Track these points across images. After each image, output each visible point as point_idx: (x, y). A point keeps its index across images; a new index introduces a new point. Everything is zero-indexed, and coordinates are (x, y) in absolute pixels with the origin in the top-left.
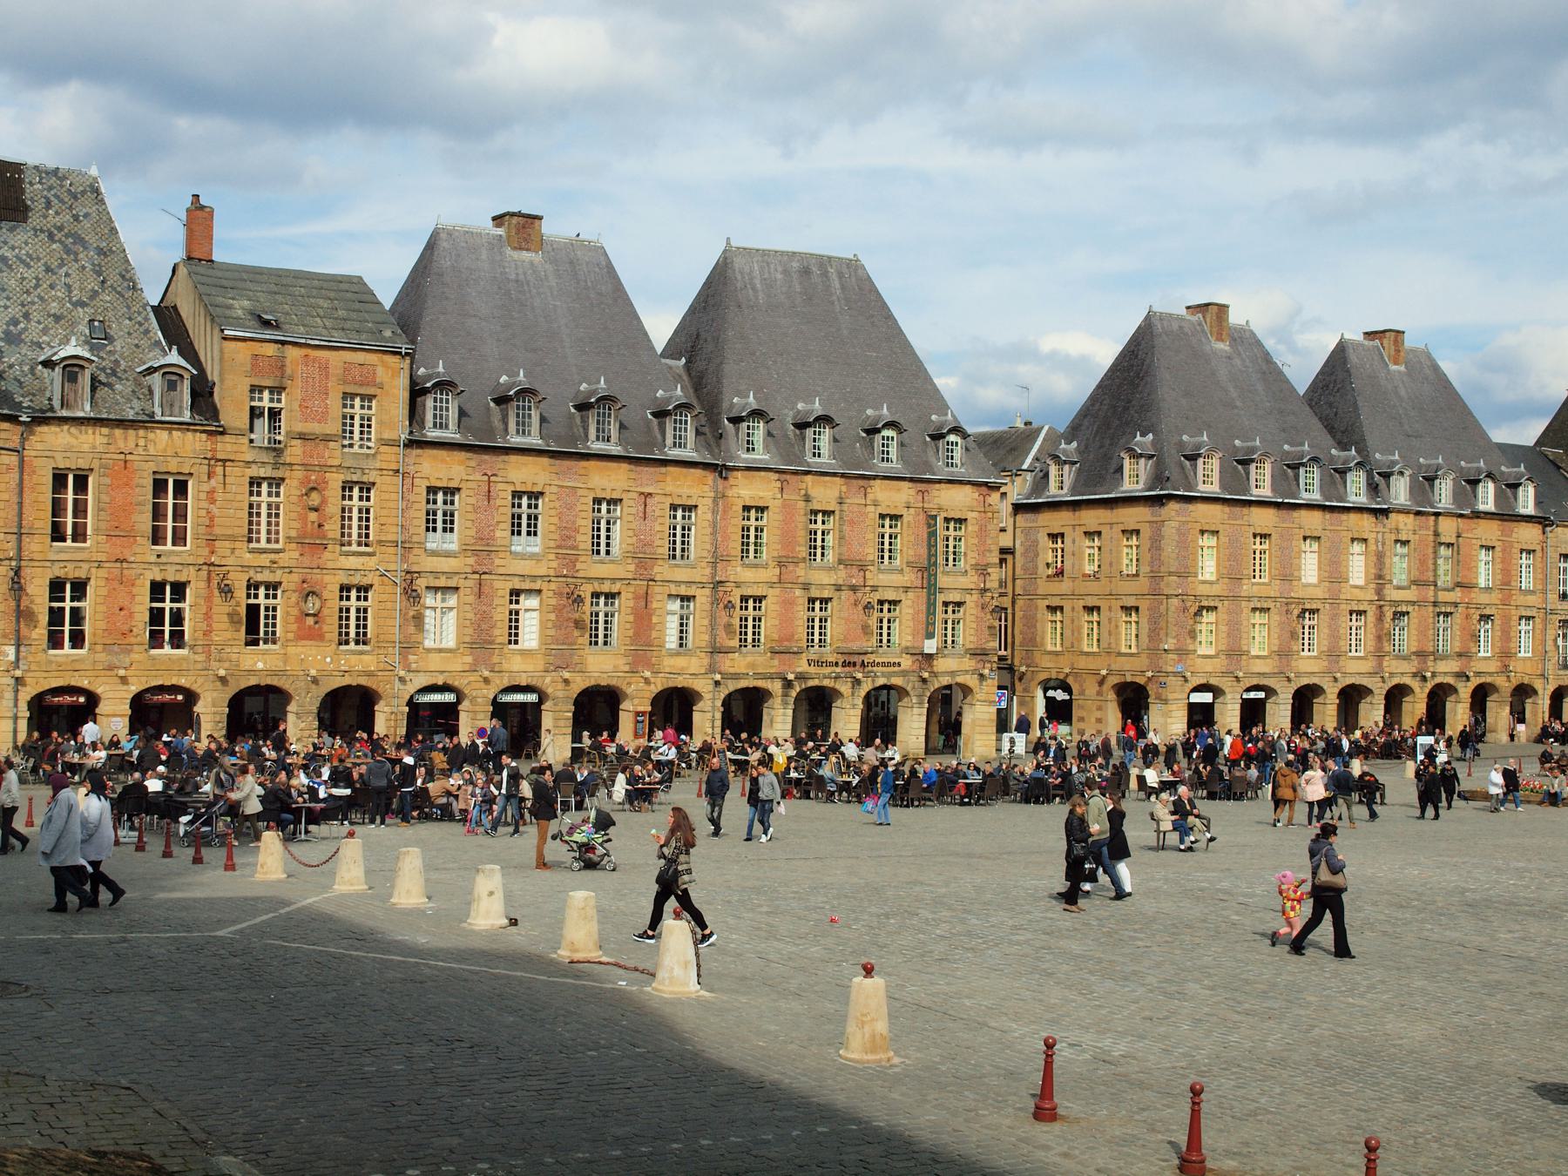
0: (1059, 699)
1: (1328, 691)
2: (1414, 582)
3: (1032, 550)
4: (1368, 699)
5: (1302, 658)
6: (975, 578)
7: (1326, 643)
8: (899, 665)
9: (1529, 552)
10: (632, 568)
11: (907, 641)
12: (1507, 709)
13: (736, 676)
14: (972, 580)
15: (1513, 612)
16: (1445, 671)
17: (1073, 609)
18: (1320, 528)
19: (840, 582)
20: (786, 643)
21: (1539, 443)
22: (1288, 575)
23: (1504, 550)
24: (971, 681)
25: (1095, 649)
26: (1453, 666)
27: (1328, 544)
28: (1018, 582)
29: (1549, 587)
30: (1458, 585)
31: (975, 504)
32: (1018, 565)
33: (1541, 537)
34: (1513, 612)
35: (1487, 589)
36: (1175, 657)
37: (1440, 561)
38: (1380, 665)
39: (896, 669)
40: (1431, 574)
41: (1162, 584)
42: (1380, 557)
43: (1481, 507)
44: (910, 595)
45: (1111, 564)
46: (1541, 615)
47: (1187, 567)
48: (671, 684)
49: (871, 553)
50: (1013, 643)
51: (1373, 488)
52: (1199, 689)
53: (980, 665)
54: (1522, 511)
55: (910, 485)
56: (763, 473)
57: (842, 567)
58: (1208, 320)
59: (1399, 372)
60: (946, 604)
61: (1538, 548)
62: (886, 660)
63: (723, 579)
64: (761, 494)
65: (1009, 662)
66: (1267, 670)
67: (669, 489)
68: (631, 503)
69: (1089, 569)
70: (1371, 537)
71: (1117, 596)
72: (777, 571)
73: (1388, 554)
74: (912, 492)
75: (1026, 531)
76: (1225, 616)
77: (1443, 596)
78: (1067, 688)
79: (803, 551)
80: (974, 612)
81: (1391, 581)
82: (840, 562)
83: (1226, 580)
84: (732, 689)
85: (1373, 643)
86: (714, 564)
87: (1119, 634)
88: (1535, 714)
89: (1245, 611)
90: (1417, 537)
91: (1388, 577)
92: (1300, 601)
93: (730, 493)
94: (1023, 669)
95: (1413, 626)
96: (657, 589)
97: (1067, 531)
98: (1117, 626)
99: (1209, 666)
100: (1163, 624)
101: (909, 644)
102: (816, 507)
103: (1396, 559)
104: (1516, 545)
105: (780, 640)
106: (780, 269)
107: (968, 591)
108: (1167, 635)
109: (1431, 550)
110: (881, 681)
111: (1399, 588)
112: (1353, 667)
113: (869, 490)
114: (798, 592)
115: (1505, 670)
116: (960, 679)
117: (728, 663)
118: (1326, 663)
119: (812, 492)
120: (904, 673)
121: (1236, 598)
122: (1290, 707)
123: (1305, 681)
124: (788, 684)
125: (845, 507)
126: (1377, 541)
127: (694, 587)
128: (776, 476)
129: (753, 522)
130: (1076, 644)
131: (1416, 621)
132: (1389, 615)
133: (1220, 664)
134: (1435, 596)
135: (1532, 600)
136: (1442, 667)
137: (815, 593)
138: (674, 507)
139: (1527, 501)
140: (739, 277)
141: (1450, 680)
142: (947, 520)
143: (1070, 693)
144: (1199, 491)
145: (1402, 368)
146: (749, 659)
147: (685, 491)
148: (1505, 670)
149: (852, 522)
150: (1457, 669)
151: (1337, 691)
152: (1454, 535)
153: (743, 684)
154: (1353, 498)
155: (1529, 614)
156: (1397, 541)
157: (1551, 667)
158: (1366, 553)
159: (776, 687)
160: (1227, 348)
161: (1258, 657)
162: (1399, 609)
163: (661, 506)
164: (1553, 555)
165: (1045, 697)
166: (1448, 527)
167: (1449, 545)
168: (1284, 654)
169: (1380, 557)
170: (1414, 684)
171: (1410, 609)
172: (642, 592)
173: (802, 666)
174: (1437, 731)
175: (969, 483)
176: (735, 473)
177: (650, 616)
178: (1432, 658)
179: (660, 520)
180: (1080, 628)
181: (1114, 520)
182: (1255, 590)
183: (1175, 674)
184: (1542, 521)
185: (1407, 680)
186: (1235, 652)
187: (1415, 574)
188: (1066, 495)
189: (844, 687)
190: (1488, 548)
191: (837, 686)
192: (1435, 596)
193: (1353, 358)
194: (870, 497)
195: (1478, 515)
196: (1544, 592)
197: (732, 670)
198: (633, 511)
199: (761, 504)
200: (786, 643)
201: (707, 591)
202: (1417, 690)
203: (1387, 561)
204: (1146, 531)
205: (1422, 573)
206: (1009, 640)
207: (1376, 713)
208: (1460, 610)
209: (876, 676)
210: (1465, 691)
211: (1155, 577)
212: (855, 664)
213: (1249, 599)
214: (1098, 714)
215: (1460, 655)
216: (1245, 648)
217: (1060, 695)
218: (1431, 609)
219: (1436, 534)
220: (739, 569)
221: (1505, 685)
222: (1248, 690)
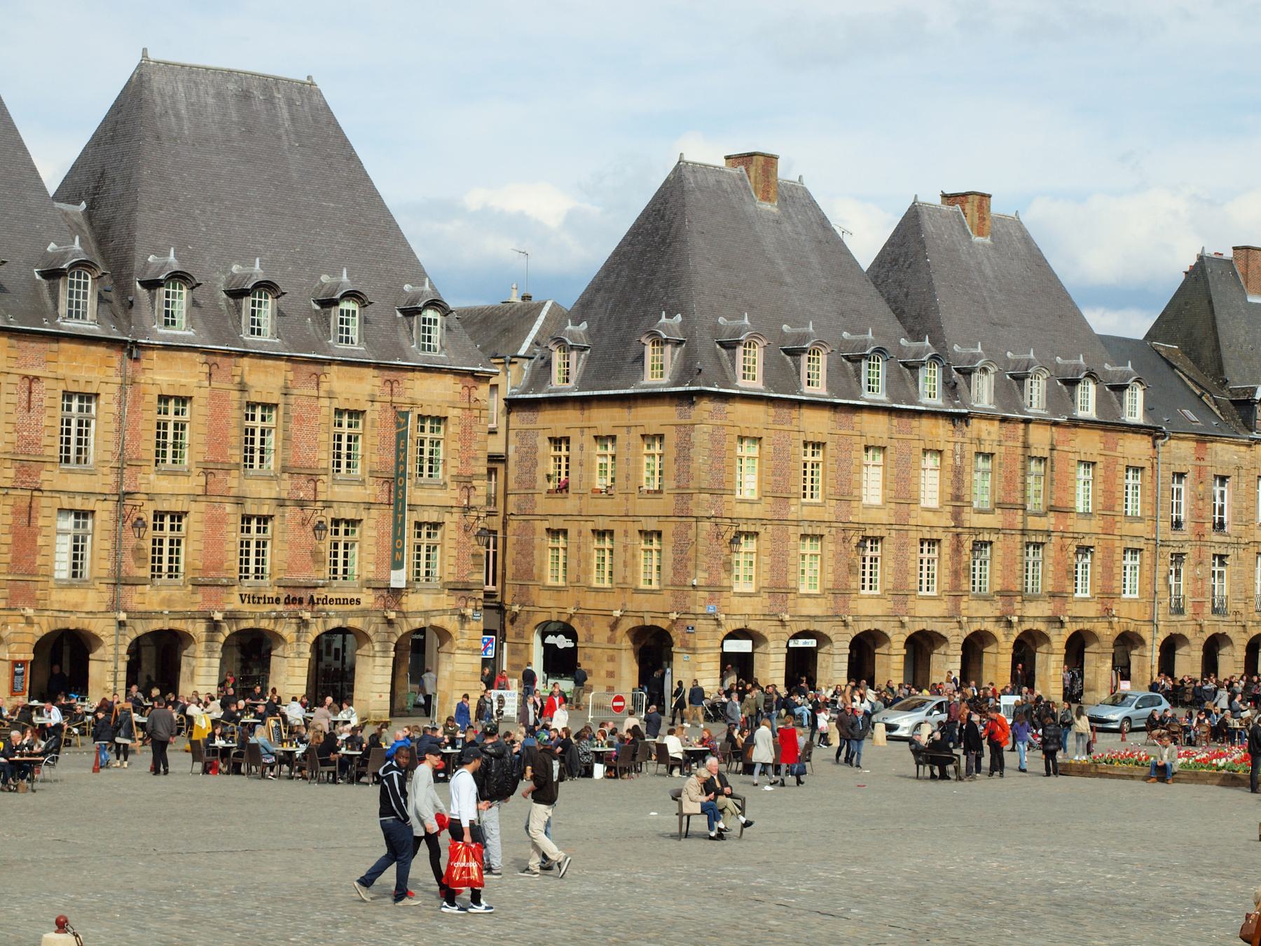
0: (561, 646)
1: (893, 639)
2: (999, 505)
3: (530, 458)
4: (942, 649)
5: (862, 597)
6: (457, 493)
7: (891, 579)
8: (358, 602)
9: (1136, 469)
10: (11, 473)
11: (369, 571)
12: (1109, 663)
13: (147, 616)
14: (451, 495)
15: (1117, 543)
16: (1035, 614)
17: (580, 533)
18: (885, 436)
19: (284, 495)
20: (212, 573)
21: (1150, 336)
22: (846, 494)
23: (1106, 467)
24: (450, 623)
25: (607, 584)
26: (1044, 609)
27: (895, 457)
28: (511, 498)
29: (1160, 513)
30: (1052, 509)
31: (458, 398)
32: (511, 477)
33: (1151, 452)
34: (1117, 543)
35: (1087, 514)
36: (706, 595)
37: (1030, 480)
39: (355, 607)
40: (1019, 495)
41: (691, 504)
42: (958, 473)
43: (1080, 414)
44: (374, 512)
45: (627, 478)
46: (1151, 547)
47: (721, 482)
48: (61, 625)
49: (324, 458)
50: (504, 575)
51: (951, 388)
52: (733, 635)
53: (461, 604)
54: (1129, 419)
55: (376, 372)
56: (185, 354)
57: (286, 476)
58: (752, 174)
59: (984, 245)
60: (419, 525)
61: (1147, 465)
62: (341, 596)
63: (131, 489)
64: (183, 381)
65: (499, 599)
67: (61, 372)
68: (11, 389)
69: (601, 483)
70: (947, 448)
71: (635, 518)
72: (202, 480)
73: (967, 469)
74: (378, 382)
75: (521, 435)
76: (768, 545)
77: (1034, 523)
78: (571, 633)
79: (236, 455)
80: (454, 535)
81: (970, 504)
82: (284, 469)
83: (770, 500)
84: (140, 631)
86: (120, 470)
87: (637, 565)
88: (1142, 669)
90: (1003, 448)
91: (967, 498)
92: (860, 526)
93: (142, 378)
94: (516, 608)
95: (997, 559)
96: (45, 502)
97: (574, 435)
98: (634, 556)
99: (748, 606)
100: (691, 553)
101: (371, 576)
102: (255, 398)
103: (977, 476)
104: (1121, 461)
105: (205, 570)
106: (212, 91)
107: (448, 508)
108: (696, 567)
109: (1019, 465)
110: (335, 623)
111: (980, 512)
112: (923, 609)
113: (322, 378)
114: (229, 508)
115: (1107, 614)
116: (436, 621)
117: (136, 598)
118: (891, 605)
119: (250, 380)
120: (365, 613)
121: (782, 521)
122: (846, 658)
123: (865, 626)
124: (214, 626)
125: (292, 400)
126: (954, 452)
127: (93, 499)
128: (203, 358)
129: (171, 417)
130: (582, 578)
131: (1000, 552)
132: (968, 545)
133: (761, 604)
134: (1024, 522)
135: (1139, 528)
136: (1032, 610)
137: (251, 509)
138: (68, 396)
139: (1134, 408)
140: (158, 100)
141: (1041, 626)
142: (422, 418)
143: (575, 640)
144: (737, 388)
145: (988, 240)
146: (164, 593)
147: (83, 375)
148: (1107, 614)
149: (300, 419)
150: (1049, 613)
151: (904, 638)
152: (1048, 447)
153: (156, 625)
154: (925, 400)
155: (1136, 546)
156: (978, 454)
157: (1162, 611)
158: (941, 468)
159: (198, 629)
160: (775, 210)
161: (808, 596)
162: (980, 538)
163: (50, 394)
164: (1165, 473)
165: (544, 644)
166: (1040, 438)
167: (1041, 460)
168: (840, 592)
169: (958, 473)
170: (998, 631)
171: (993, 538)
172: (25, 504)
173: (233, 602)
174: (1025, 689)
175: (450, 371)
176: (149, 353)
177: (34, 536)
178: (1019, 598)
179: (49, 412)
180: (588, 558)
181: (632, 422)
182: (806, 513)
183: (707, 616)
184: (1152, 432)
185: (989, 626)
186: (779, 590)
187: (1000, 495)
188: (572, 390)
189: (287, 631)
190: (1089, 464)
191: (278, 629)
192: (1024, 522)
193: (928, 226)
194: (324, 386)
195: (1075, 423)
196: (1154, 519)
197: (141, 608)
198: (14, 399)
199: (182, 393)
200: (212, 573)
201: (110, 505)
202: (1001, 638)
203: (967, 479)
204: (672, 437)
205: (1008, 493)
206: (499, 572)
208: (1053, 539)
209: (328, 616)
210: (1059, 640)
211: (683, 494)
212: (301, 601)
213: (798, 522)
214: (610, 666)
215: (1053, 595)
216: (792, 585)
217: (562, 642)
218: (1018, 538)
219: (1026, 446)
220: (152, 477)
222: (796, 636)
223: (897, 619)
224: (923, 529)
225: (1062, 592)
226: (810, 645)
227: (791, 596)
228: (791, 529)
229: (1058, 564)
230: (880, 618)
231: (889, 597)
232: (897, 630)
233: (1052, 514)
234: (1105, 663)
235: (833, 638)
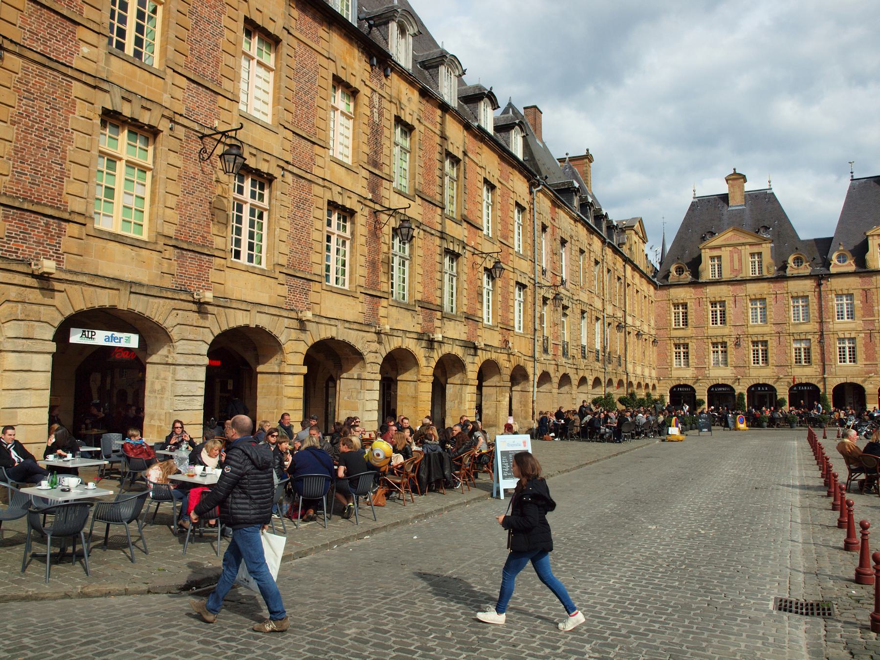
4: (355, 372)
38: (374, 312)
61: (527, 207)
66: (142, 275)
85: (362, 271)
89: (81, 108)
95: (418, 260)
123: (239, 319)
141: (458, 351)
150: (464, 337)
151: (303, 348)
170: (419, 350)
185: (411, 344)
202: (422, 362)
205: (429, 183)
207: (368, 395)
216: (76, 205)
218: (438, 241)
221: (506, 365)
223: (293, 315)
224: (333, 187)
225: (474, 316)
226: (123, 344)
227: (72, 229)
228: (77, 89)
229: (471, 282)
230: (266, 310)
231: (282, 278)
232: (294, 334)
233: (465, 225)
234: (505, 396)
235: (175, 334)
